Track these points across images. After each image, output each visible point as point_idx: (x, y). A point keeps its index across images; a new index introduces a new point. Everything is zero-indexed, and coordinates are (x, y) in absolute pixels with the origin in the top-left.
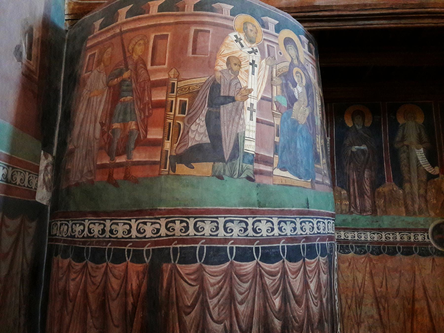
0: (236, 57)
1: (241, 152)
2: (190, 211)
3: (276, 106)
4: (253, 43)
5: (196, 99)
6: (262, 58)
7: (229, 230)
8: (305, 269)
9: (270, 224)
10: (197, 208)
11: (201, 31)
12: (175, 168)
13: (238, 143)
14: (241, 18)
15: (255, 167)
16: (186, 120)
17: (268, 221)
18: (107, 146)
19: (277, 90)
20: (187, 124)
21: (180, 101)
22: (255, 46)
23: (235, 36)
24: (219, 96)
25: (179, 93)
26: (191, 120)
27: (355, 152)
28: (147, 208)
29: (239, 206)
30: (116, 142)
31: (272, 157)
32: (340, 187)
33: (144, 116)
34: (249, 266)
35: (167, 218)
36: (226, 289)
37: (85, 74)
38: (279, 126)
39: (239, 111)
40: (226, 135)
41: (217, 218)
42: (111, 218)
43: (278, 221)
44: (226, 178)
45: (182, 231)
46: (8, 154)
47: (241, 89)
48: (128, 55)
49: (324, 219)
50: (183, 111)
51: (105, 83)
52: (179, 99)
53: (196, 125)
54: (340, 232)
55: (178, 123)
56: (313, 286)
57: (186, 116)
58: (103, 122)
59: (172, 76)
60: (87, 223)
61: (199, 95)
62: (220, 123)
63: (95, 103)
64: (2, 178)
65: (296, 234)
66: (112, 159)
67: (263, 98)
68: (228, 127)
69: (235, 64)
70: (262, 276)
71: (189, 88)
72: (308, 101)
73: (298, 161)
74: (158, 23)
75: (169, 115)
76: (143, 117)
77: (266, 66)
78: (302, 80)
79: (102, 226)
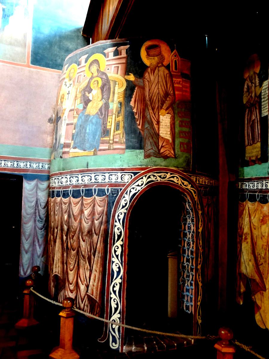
8: (82, 202)
17: (66, 177)
19: (78, 101)
34: (59, 199)
36: (53, 210)
44: (56, 158)
49: (105, 173)
56: (86, 212)
65: (78, 184)
67: (70, 111)
70: (62, 204)
72: (103, 96)
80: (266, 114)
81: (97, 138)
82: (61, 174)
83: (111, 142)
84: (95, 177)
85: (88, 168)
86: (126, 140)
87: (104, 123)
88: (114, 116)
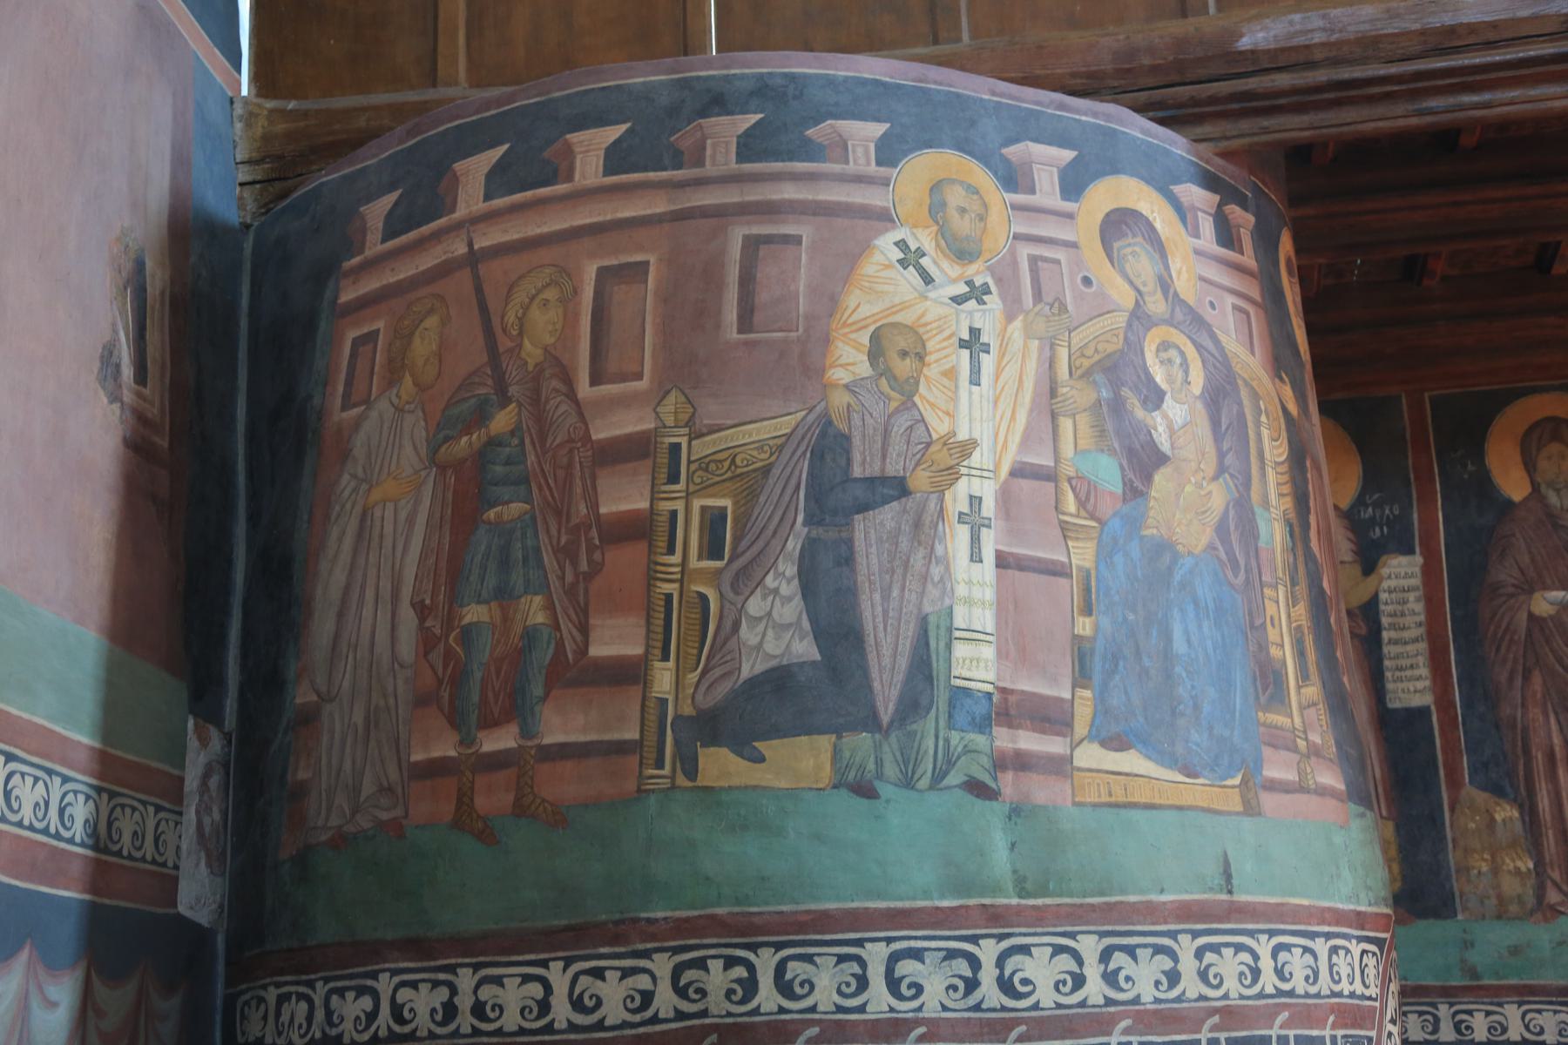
0: (906, 326)
1: (942, 688)
2: (756, 920)
3: (1076, 496)
4: (971, 262)
5: (762, 499)
6: (1010, 317)
7: (909, 987)
9: (1065, 962)
10: (784, 908)
11: (769, 239)
12: (697, 761)
13: (929, 656)
14: (920, 168)
15: (998, 743)
16: (727, 577)
17: (1058, 950)
18: (445, 695)
20: (730, 595)
21: (704, 509)
22: (978, 273)
23: (896, 244)
24: (848, 479)
25: (699, 480)
26: (745, 579)
27: (1551, 617)
28: (604, 917)
29: (942, 897)
30: (478, 675)
31: (1067, 695)
32: (1484, 789)
33: (577, 575)
35: (676, 951)
37: (339, 416)
38: (1093, 573)
39: (924, 530)
40: (881, 627)
41: (859, 943)
42: (474, 960)
43: (1101, 947)
44: (885, 790)
45: (734, 998)
46: (97, 745)
47: (929, 445)
48: (504, 343)
49: (1312, 936)
50: (713, 548)
51: (423, 452)
52: (697, 504)
53: (764, 597)
54: (1500, 1005)
55: (698, 592)
57: (727, 564)
58: (423, 601)
59: (670, 421)
60: (384, 984)
61: (771, 481)
62: (855, 582)
63: (389, 529)
64: (84, 836)
65: (1179, 999)
66: (467, 741)
67: (1019, 472)
68: (886, 597)
69: (904, 354)
71: (733, 461)
72: (1221, 455)
73: (1181, 707)
74: (609, 217)
75: (664, 565)
76: (569, 578)
77: (1025, 342)
78: (1186, 372)
79: (444, 993)
80: (1427, 700)
81: (1238, 707)
82: (996, 917)
83: (1301, 744)
84: (1274, 955)
85: (1230, 892)
86: (1339, 745)
87: (1258, 622)
88: (1281, 589)
